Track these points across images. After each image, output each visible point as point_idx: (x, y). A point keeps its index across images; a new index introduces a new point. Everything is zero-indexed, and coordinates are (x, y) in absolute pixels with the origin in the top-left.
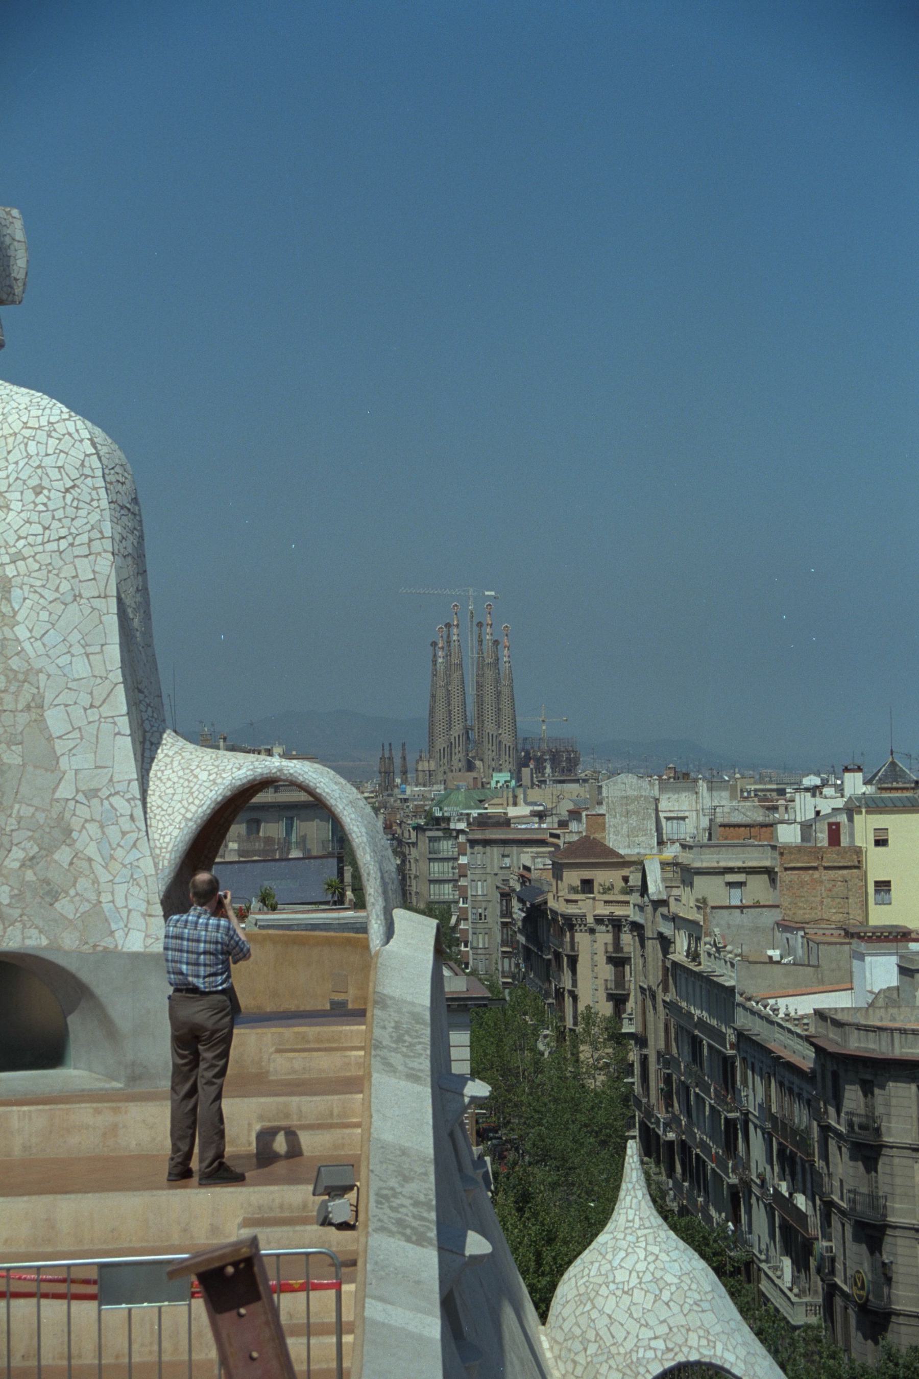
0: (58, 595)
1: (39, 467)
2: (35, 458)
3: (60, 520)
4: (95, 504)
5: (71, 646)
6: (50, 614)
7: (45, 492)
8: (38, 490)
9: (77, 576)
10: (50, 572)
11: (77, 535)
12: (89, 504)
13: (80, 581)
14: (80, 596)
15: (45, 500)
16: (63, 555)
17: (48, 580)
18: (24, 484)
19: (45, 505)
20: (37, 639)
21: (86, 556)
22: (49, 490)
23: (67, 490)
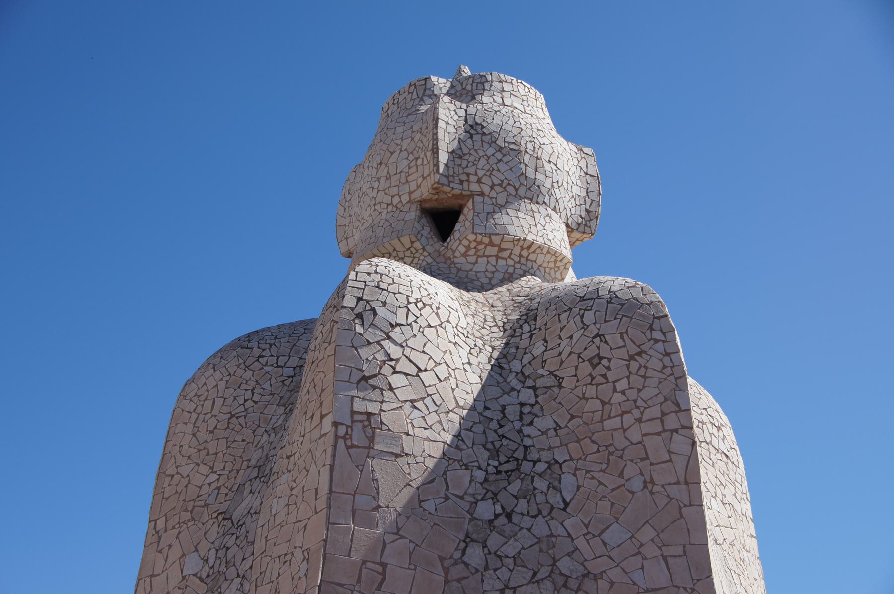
0: (623, 481)
1: (598, 335)
2: (592, 327)
3: (623, 393)
4: (668, 371)
5: (642, 545)
6: (613, 504)
7: (605, 362)
8: (596, 360)
9: (647, 458)
10: (611, 454)
11: (645, 408)
12: (661, 372)
13: (652, 464)
14: (652, 482)
15: (605, 371)
16: (628, 433)
17: (608, 464)
18: (579, 357)
19: (604, 376)
20: (594, 536)
21: (658, 434)
22: (610, 360)
23: (632, 358)
